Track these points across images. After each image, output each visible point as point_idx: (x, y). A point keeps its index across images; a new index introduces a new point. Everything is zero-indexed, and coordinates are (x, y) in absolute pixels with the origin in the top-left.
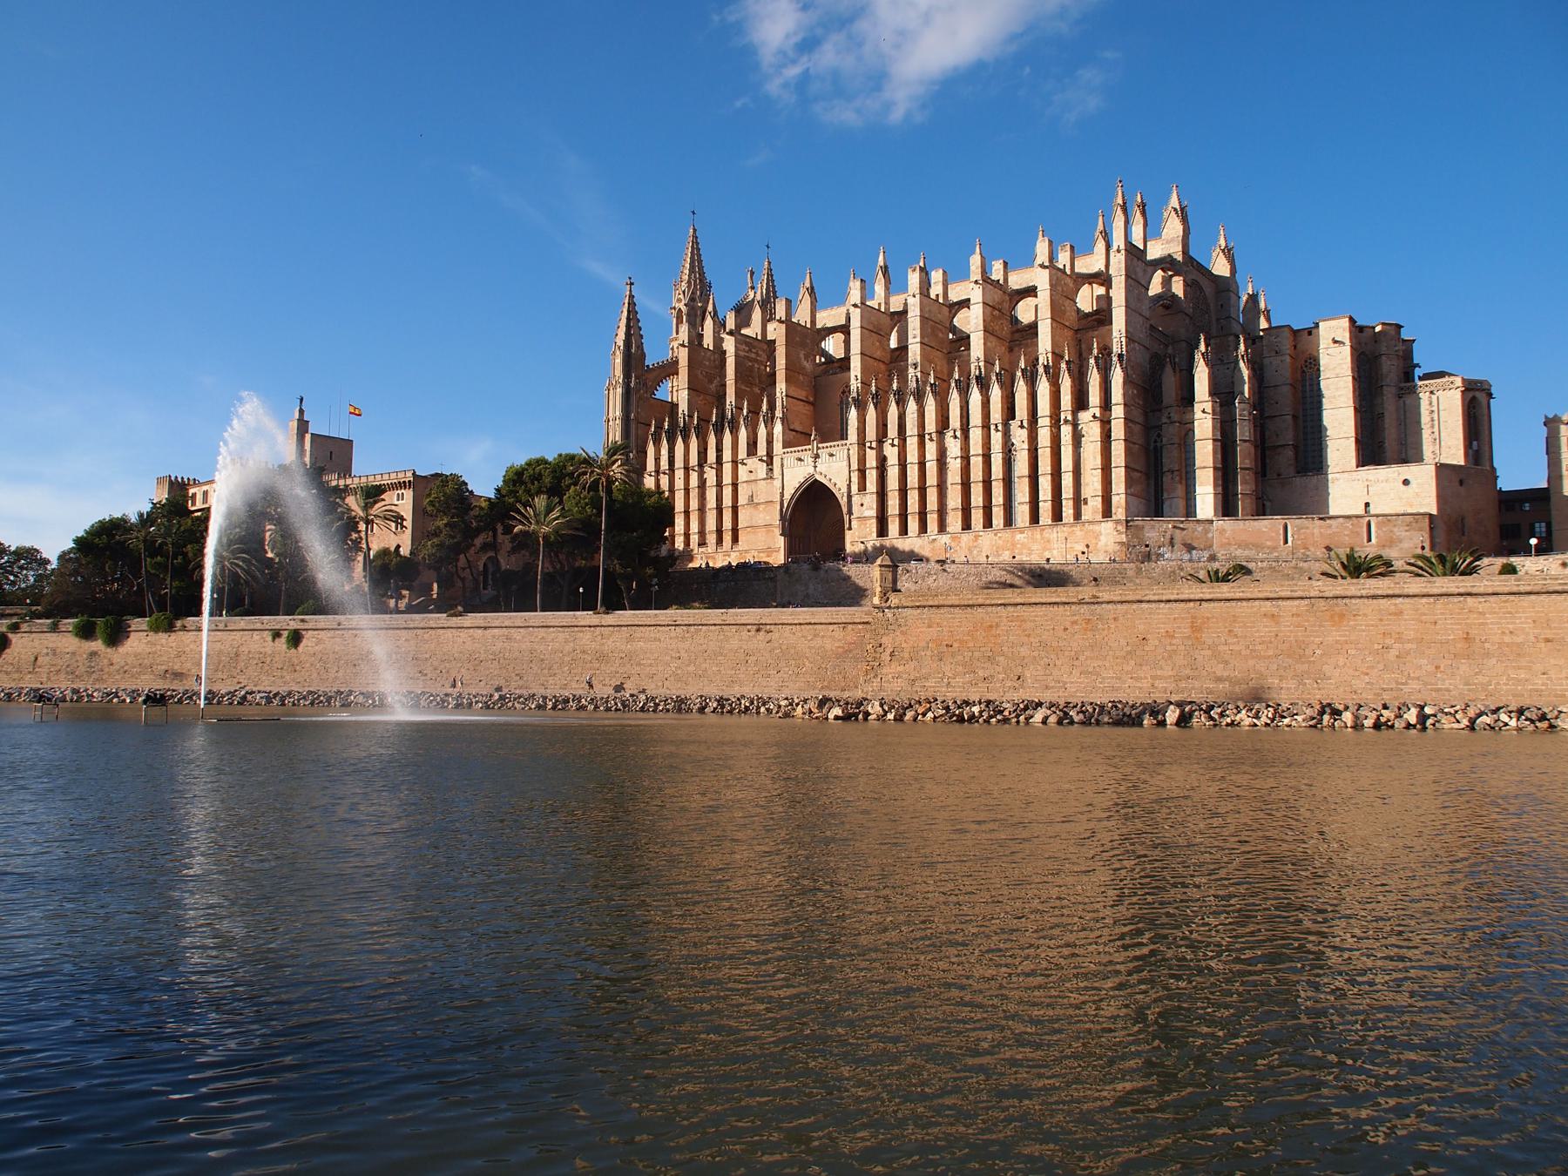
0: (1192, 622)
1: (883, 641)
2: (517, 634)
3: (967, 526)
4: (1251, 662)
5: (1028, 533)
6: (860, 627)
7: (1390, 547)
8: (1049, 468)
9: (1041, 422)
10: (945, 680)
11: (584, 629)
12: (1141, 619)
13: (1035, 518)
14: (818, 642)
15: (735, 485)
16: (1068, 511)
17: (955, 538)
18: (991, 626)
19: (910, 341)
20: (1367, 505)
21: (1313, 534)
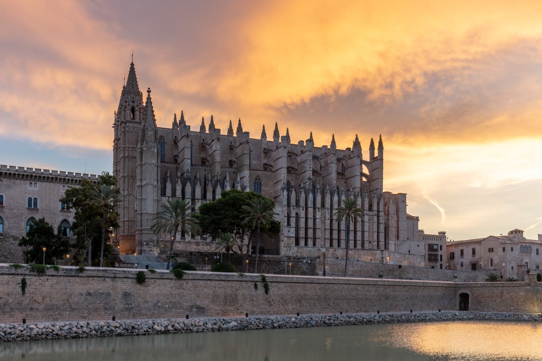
2: (359, 288)
5: (353, 251)
8: (361, 229)
11: (380, 286)
13: (355, 245)
16: (367, 245)
17: (327, 249)
20: (409, 251)
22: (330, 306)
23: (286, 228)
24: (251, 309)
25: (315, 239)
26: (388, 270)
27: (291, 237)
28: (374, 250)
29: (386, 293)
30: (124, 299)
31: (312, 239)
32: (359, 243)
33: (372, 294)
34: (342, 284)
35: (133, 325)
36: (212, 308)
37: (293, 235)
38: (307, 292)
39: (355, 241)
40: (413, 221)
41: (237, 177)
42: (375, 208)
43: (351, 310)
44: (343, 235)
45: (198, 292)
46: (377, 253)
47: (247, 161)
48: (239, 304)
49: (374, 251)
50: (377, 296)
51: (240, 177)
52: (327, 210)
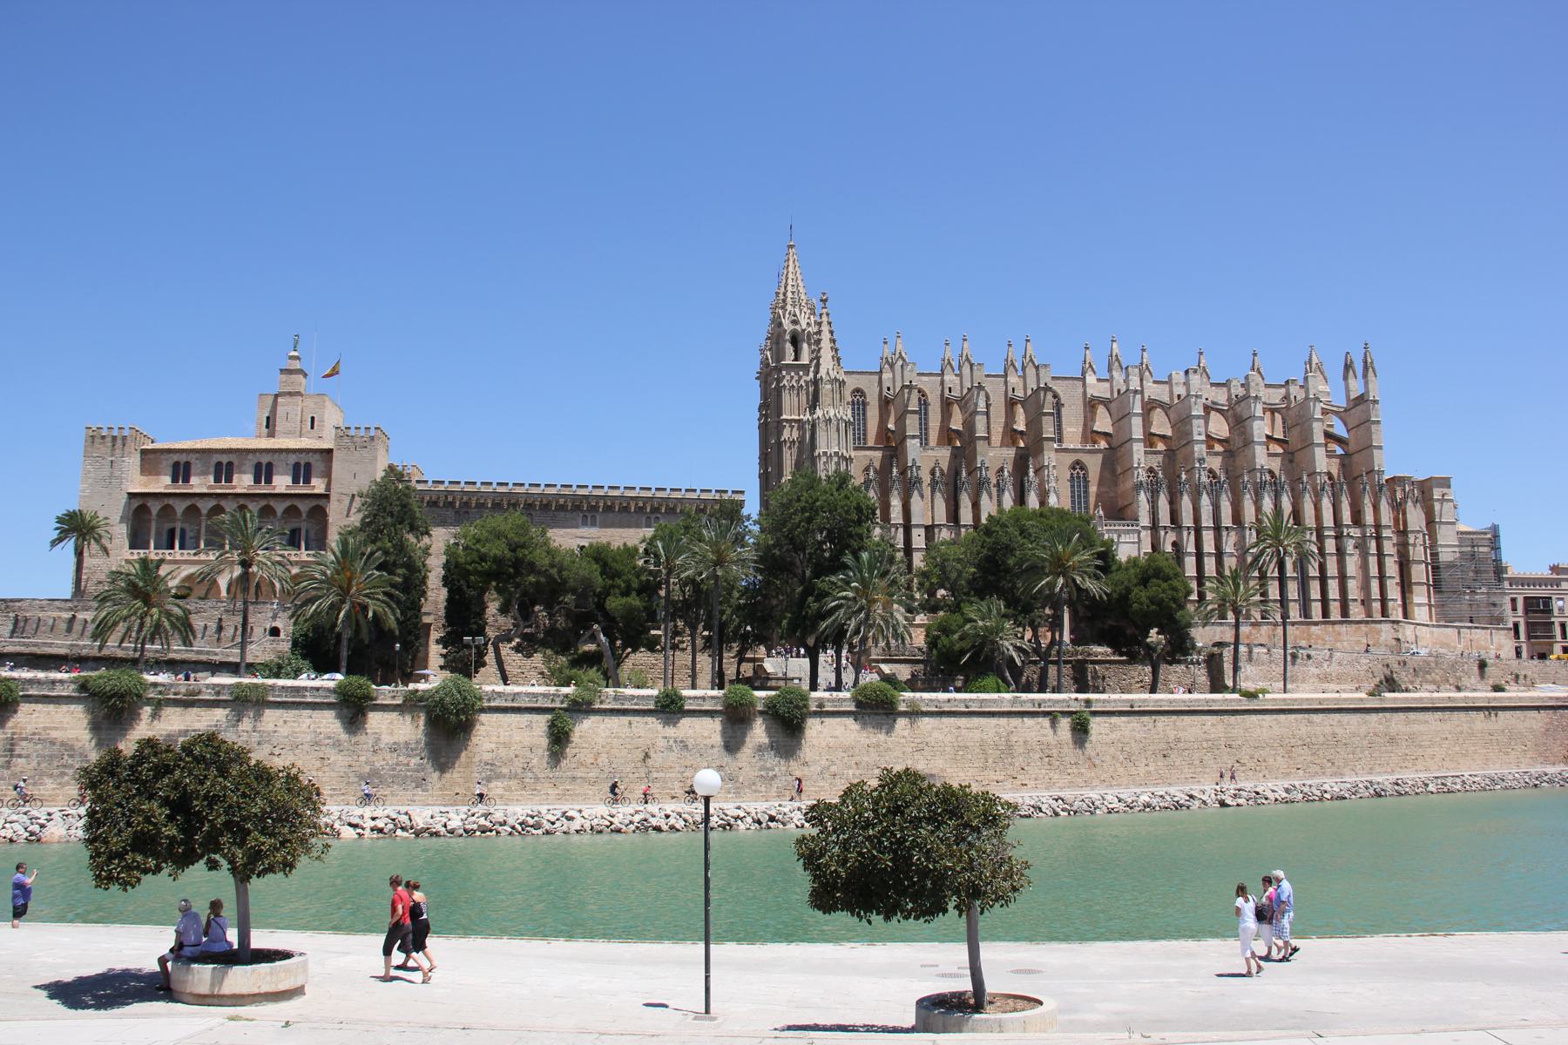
13: (1325, 613)
16: (1356, 611)
19: (1196, 437)
22: (1243, 765)
24: (1047, 777)
30: (757, 758)
32: (1335, 609)
35: (773, 813)
36: (954, 775)
38: (1181, 734)
39: (1325, 601)
41: (1028, 468)
42: (1367, 518)
45: (919, 741)
48: (1017, 764)
50: (1365, 736)
51: (1034, 468)
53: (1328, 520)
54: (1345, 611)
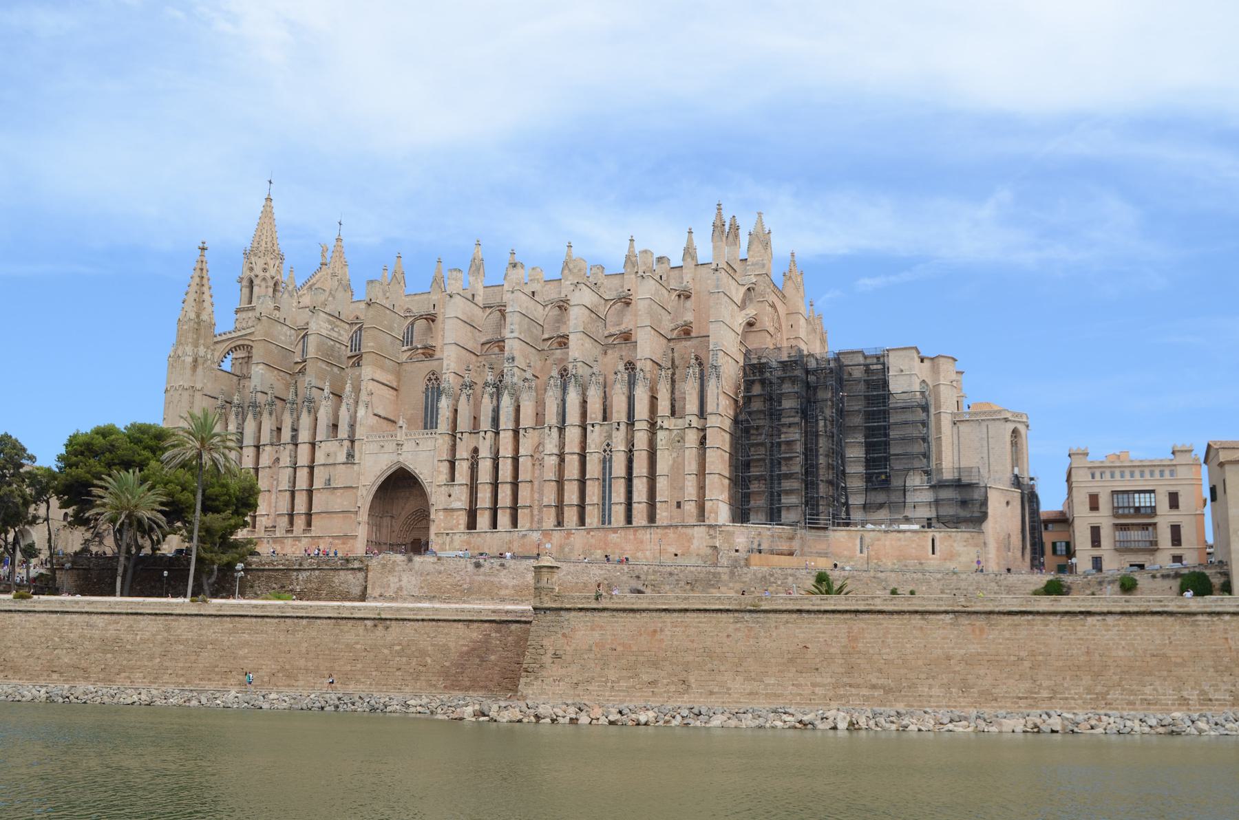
0: (849, 632)
1: (544, 643)
2: (99, 621)
3: (560, 523)
4: (903, 671)
5: (623, 533)
6: (487, 625)
7: (950, 560)
9: (638, 426)
10: (609, 684)
12: (801, 628)
13: (629, 519)
14: (441, 640)
15: (311, 468)
16: (662, 514)
17: (546, 533)
18: (655, 631)
21: (885, 546)
23: (444, 487)
25: (514, 510)
26: (682, 583)
27: (453, 510)
28: (686, 526)
29: (202, 635)
31: (508, 511)
32: (640, 511)
33: (141, 638)
34: (42, 612)
37: (460, 504)
40: (984, 424)
43: (48, 676)
44: (590, 493)
46: (695, 535)
47: (369, 344)
49: (684, 530)
52: (547, 430)
53: (642, 411)
54: (652, 518)
